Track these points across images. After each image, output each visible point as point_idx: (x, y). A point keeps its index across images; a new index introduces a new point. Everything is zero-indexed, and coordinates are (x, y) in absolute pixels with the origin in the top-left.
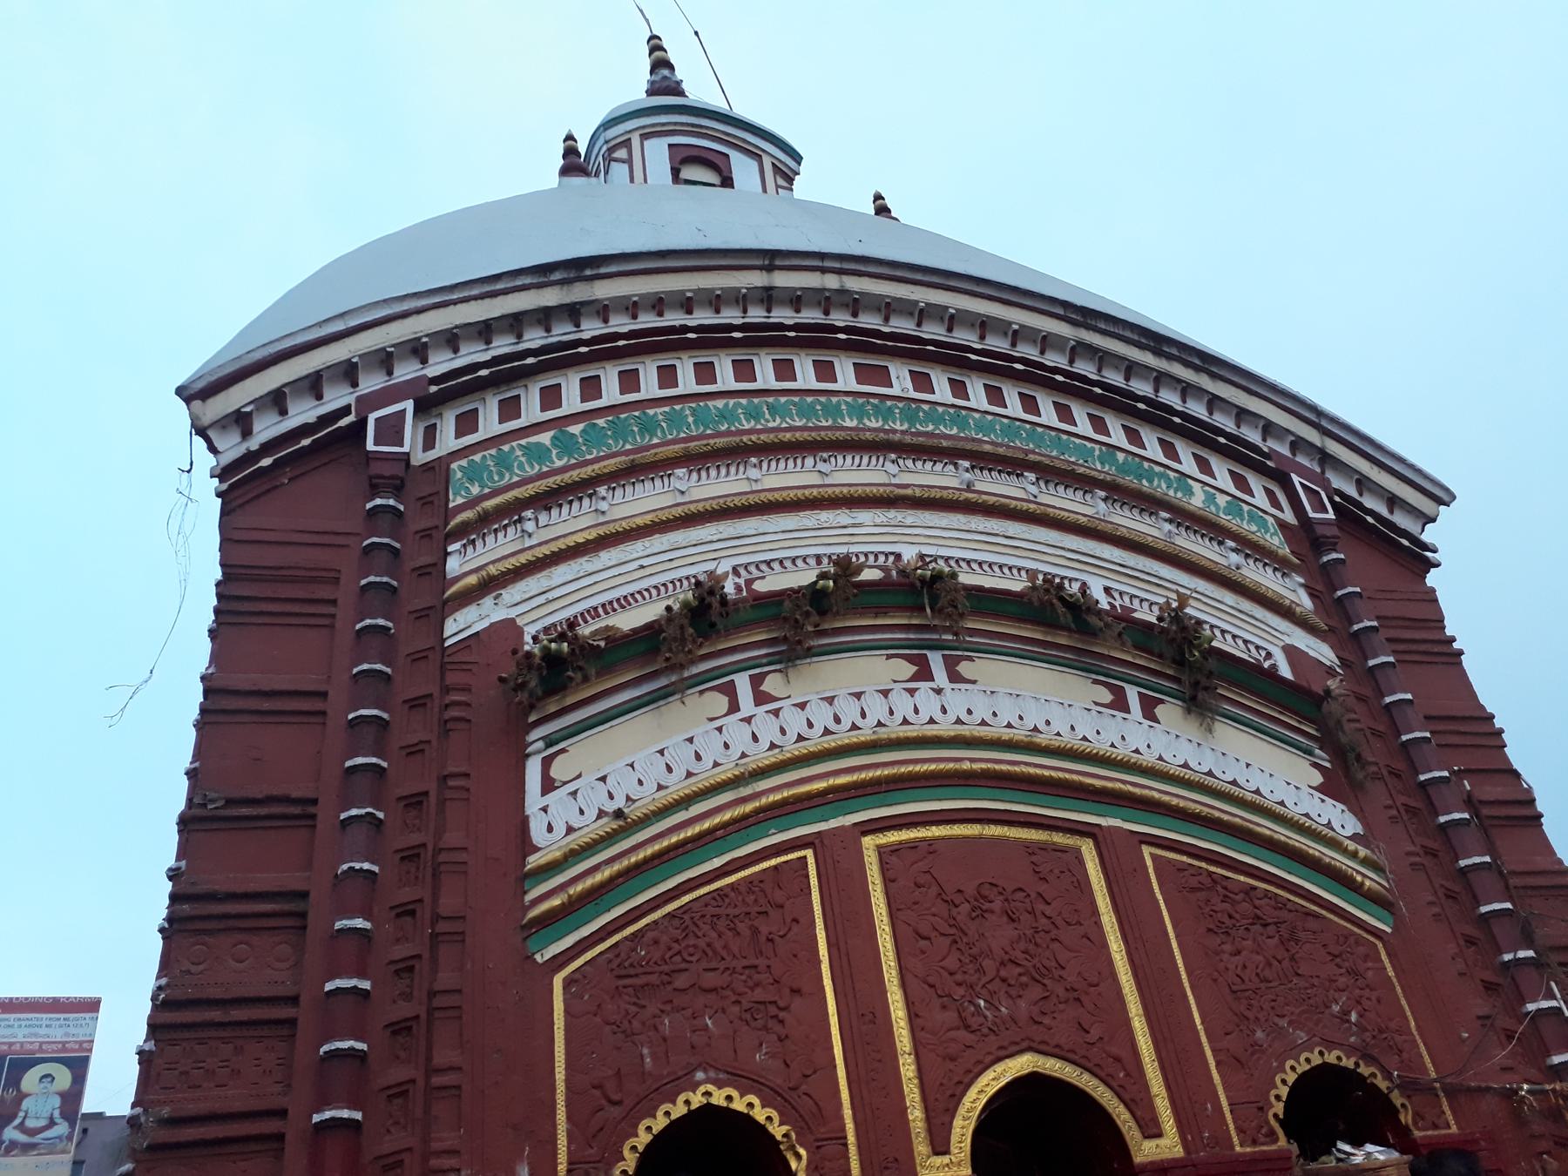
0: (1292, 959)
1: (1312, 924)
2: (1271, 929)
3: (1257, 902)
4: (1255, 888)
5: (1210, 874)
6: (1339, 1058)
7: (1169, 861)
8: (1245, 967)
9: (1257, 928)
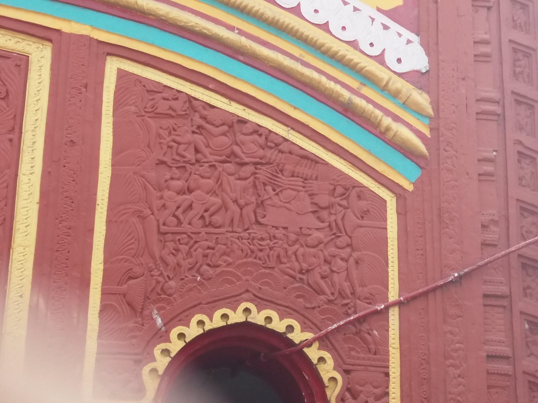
0: (261, 204)
1: (304, 169)
2: (248, 170)
3: (241, 137)
4: (243, 121)
5: (191, 99)
6: (269, 319)
7: (139, 80)
8: (190, 207)
9: (230, 167)
